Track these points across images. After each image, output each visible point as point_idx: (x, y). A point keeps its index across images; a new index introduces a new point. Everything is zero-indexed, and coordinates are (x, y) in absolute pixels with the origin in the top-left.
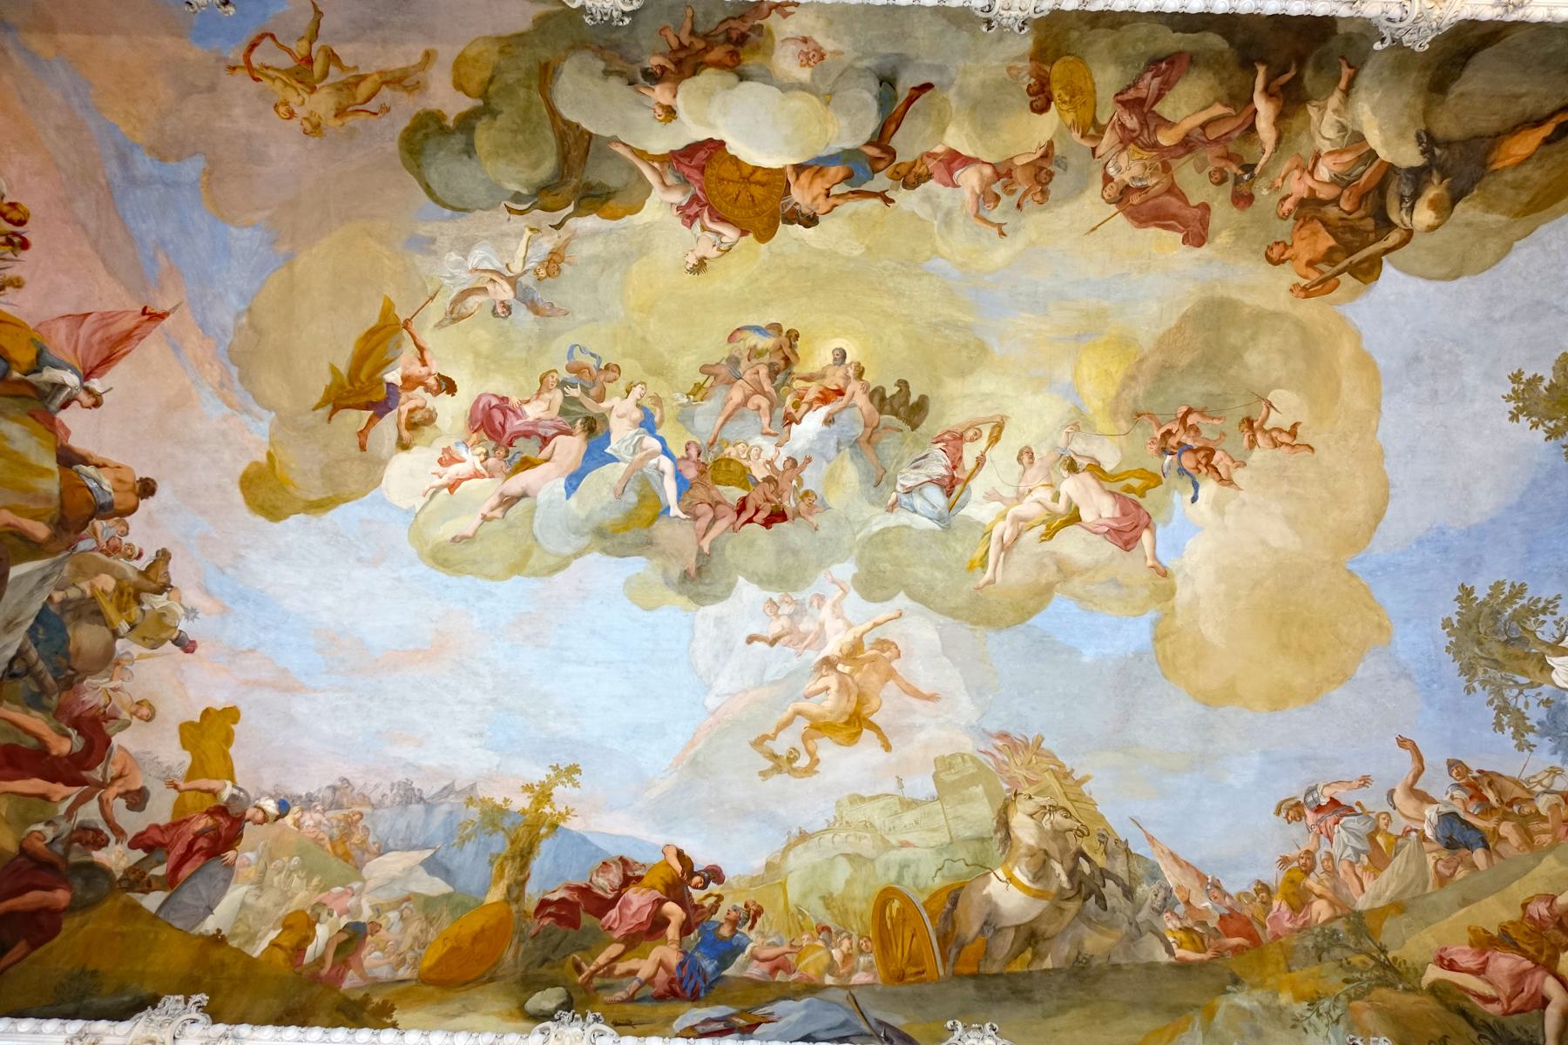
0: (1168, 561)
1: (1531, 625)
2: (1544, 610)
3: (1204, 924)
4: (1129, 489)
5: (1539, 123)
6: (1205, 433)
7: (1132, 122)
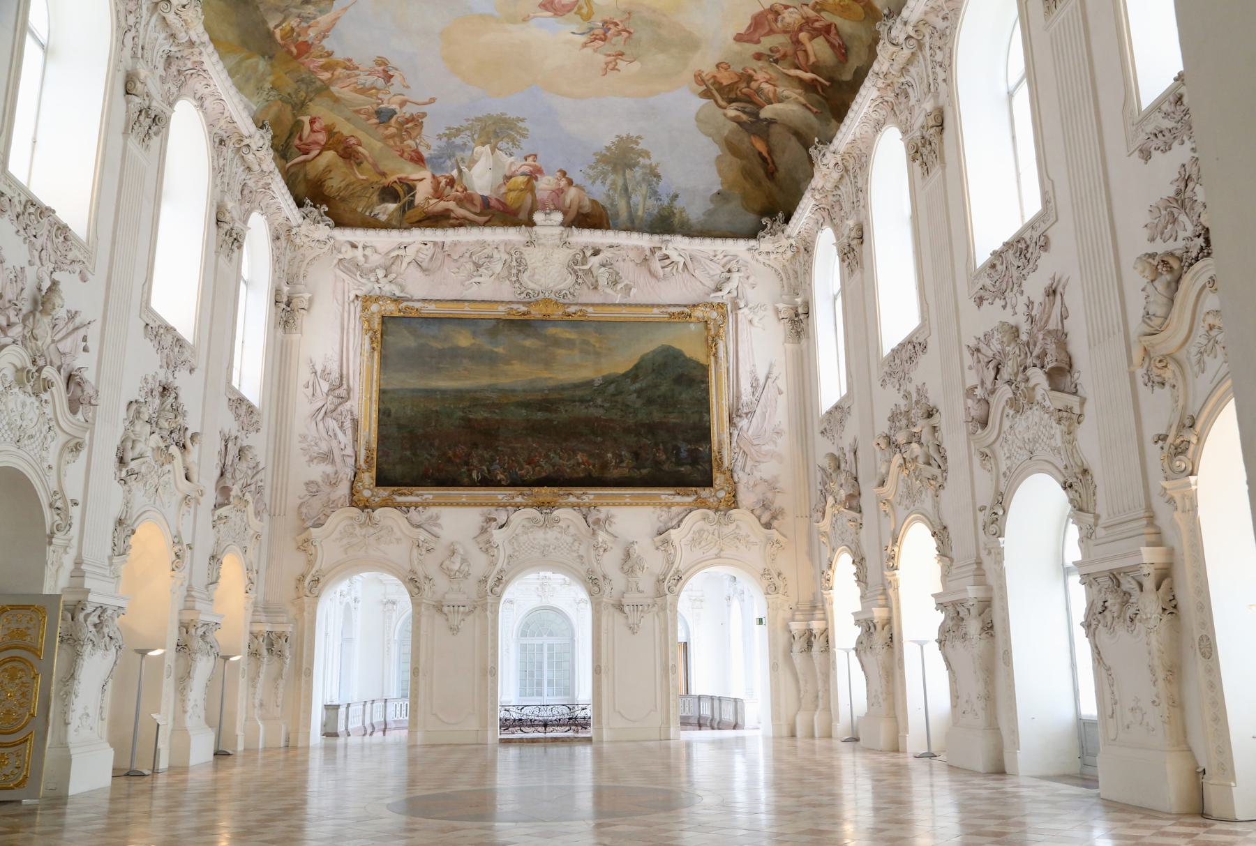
0: (532, 22)
1: (506, 140)
2: (514, 144)
3: (299, 35)
4: (580, 8)
5: (769, 154)
6: (615, 39)
7: (817, 25)
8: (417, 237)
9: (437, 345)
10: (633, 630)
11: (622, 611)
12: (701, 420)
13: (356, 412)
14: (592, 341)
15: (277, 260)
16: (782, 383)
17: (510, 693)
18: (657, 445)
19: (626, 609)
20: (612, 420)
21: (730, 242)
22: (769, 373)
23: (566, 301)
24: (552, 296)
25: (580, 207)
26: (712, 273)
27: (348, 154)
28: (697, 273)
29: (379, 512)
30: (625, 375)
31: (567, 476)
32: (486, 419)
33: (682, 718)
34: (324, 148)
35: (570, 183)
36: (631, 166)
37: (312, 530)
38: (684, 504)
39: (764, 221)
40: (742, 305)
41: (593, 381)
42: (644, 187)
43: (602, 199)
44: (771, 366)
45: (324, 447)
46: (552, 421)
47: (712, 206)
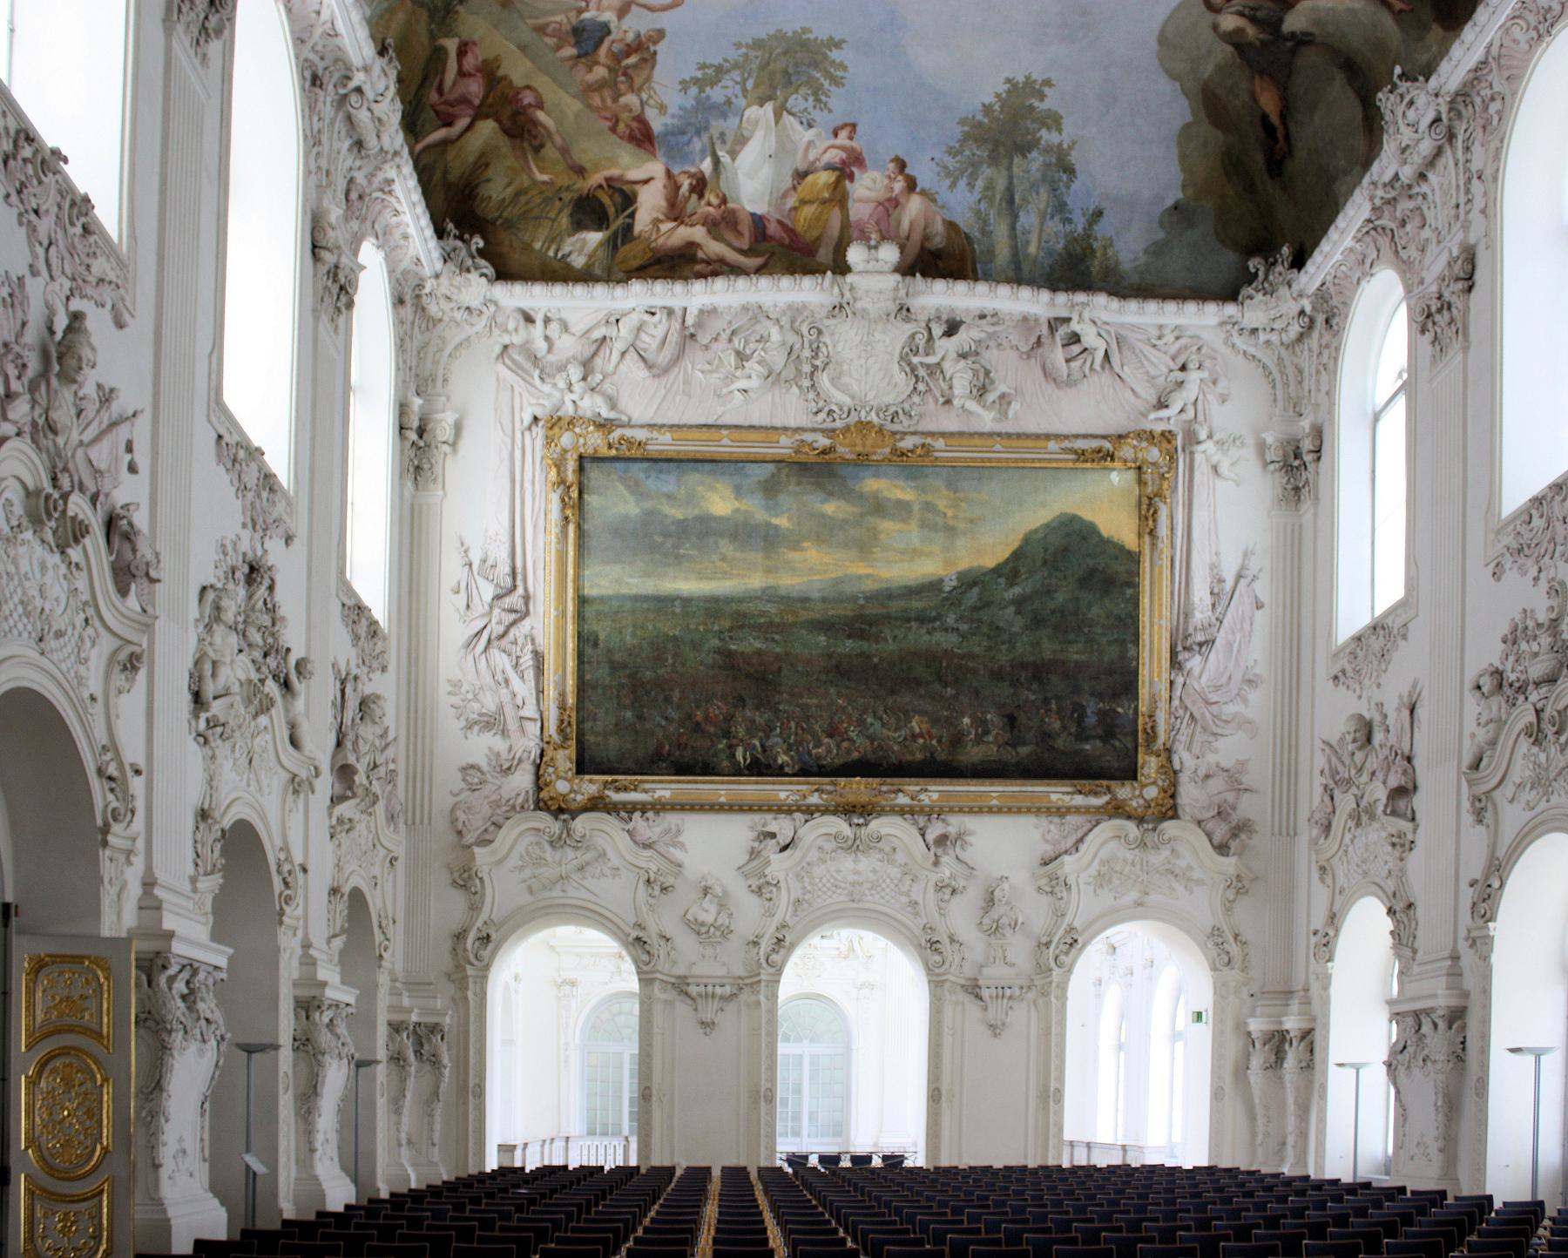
8: (638, 296)
9: (675, 512)
10: (995, 1029)
11: (979, 997)
12: (1123, 657)
13: (539, 640)
14: (941, 504)
15: (401, 346)
16: (1262, 589)
18: (1046, 701)
19: (985, 993)
20: (971, 656)
21: (1191, 307)
22: (1243, 567)
23: (896, 427)
24: (873, 417)
25: (926, 238)
26: (1153, 372)
27: (521, 128)
28: (1126, 373)
29: (582, 824)
30: (997, 571)
31: (894, 759)
32: (759, 653)
34: (479, 114)
35: (911, 185)
36: (1024, 149)
37: (476, 850)
39: (1254, 264)
40: (1203, 435)
41: (941, 581)
42: (1044, 193)
43: (965, 220)
44: (1245, 555)
45: (490, 704)
46: (870, 657)
47: (1161, 235)
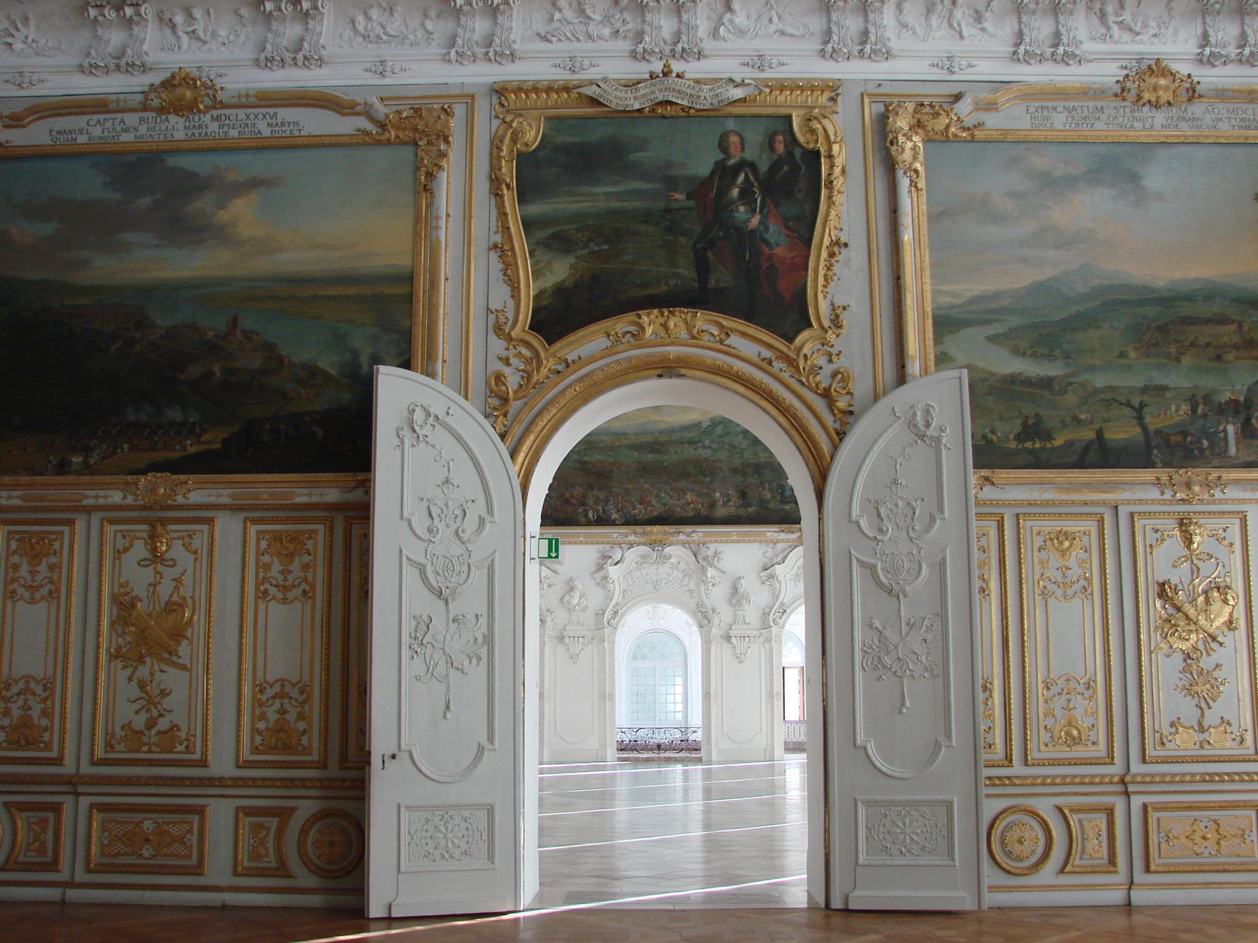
17: (625, 717)
18: (762, 484)
32: (600, 461)
33: (785, 743)
38: (788, 541)
